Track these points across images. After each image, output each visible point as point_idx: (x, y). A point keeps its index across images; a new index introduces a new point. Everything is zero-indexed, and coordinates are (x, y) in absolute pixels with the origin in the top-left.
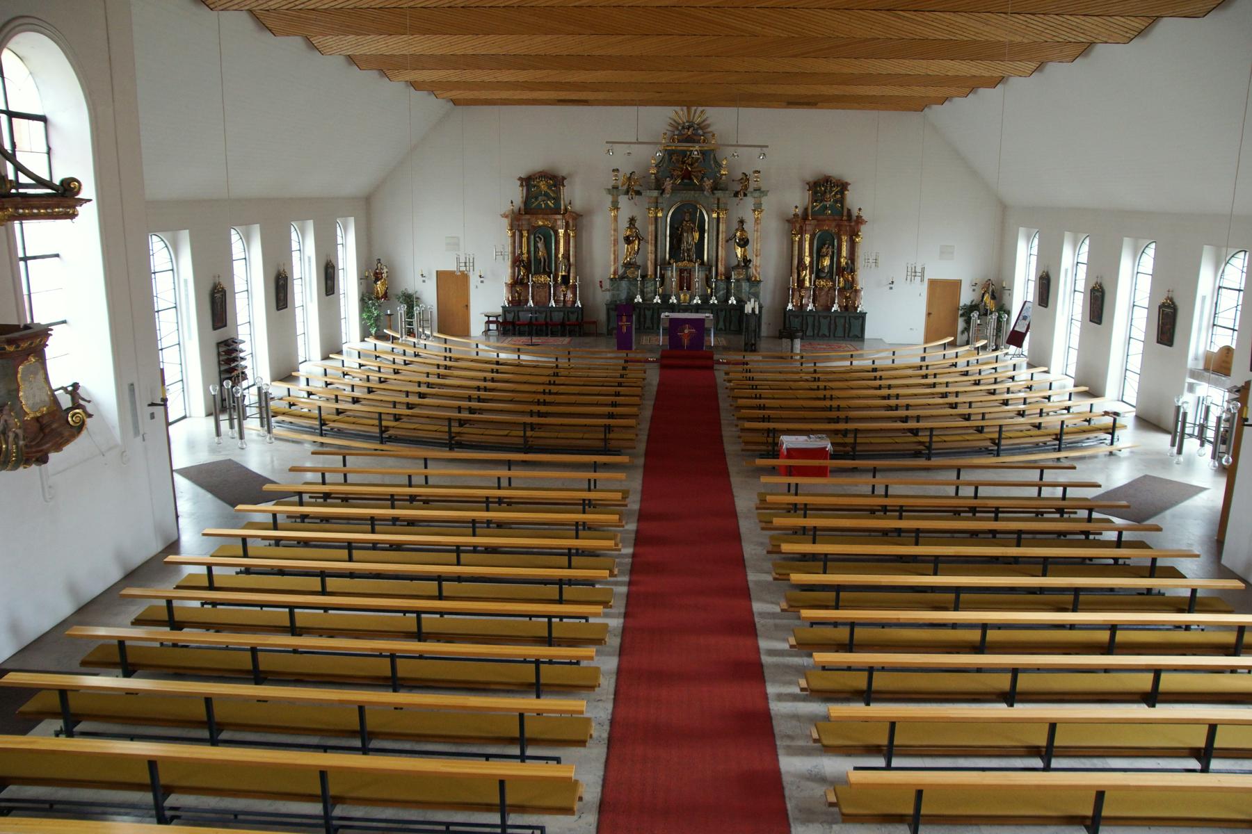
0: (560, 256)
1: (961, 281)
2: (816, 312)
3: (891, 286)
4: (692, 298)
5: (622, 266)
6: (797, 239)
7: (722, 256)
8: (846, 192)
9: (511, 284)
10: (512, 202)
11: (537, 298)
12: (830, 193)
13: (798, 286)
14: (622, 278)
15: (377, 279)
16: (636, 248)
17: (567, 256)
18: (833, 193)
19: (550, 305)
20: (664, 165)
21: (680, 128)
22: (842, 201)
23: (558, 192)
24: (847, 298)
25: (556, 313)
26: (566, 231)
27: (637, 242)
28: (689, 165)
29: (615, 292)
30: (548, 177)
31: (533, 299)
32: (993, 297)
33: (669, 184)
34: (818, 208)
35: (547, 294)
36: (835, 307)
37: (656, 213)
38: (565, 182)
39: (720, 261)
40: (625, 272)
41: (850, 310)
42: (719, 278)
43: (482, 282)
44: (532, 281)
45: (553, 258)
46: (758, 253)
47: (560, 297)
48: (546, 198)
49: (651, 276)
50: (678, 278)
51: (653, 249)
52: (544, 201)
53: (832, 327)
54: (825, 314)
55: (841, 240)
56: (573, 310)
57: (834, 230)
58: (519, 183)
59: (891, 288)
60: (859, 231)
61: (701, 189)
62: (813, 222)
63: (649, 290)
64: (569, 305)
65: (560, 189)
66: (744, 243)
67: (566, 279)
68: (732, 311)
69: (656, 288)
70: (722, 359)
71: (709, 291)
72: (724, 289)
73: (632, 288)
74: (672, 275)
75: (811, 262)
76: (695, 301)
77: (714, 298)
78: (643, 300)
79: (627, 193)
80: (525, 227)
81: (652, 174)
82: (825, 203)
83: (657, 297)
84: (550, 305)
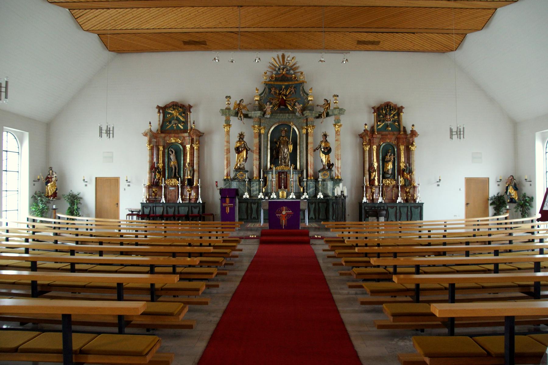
0: (187, 165)
1: (488, 178)
2: (385, 203)
3: (438, 183)
4: (288, 194)
5: (234, 171)
6: (368, 149)
7: (311, 162)
8: (402, 114)
9: (149, 186)
10: (150, 123)
11: (169, 197)
12: (390, 115)
13: (369, 184)
14: (234, 179)
15: (47, 183)
16: (245, 156)
17: (192, 164)
18: (392, 115)
19: (178, 202)
20: (266, 96)
21: (277, 69)
22: (399, 121)
23: (186, 117)
24: (406, 193)
25: (183, 208)
26: (191, 146)
27: (245, 152)
28: (284, 95)
30: (178, 106)
31: (165, 197)
32: (516, 188)
33: (268, 108)
34: (381, 126)
35: (177, 194)
36: (399, 200)
37: (260, 130)
38: (191, 110)
39: (309, 165)
40: (236, 175)
41: (410, 202)
42: (309, 178)
43: (129, 185)
44: (165, 183)
45: (182, 167)
46: (339, 158)
47: (187, 196)
48: (177, 122)
49: (256, 177)
50: (277, 179)
51: (258, 157)
52: (176, 124)
53: (398, 215)
54: (392, 205)
55: (400, 149)
56: (196, 205)
57: (394, 143)
58: (157, 110)
59: (438, 185)
60: (413, 142)
61: (294, 112)
62: (378, 136)
63: (254, 188)
64: (192, 201)
65: (188, 114)
66: (328, 151)
67: (191, 182)
68: (320, 204)
69: (260, 187)
70: (318, 235)
72: (313, 188)
74: (272, 178)
75: (379, 166)
76: (291, 197)
77: (305, 194)
78: (250, 196)
79: (236, 114)
80: (162, 143)
81: (256, 100)
82: (386, 122)
83: (261, 194)
84: (178, 202)
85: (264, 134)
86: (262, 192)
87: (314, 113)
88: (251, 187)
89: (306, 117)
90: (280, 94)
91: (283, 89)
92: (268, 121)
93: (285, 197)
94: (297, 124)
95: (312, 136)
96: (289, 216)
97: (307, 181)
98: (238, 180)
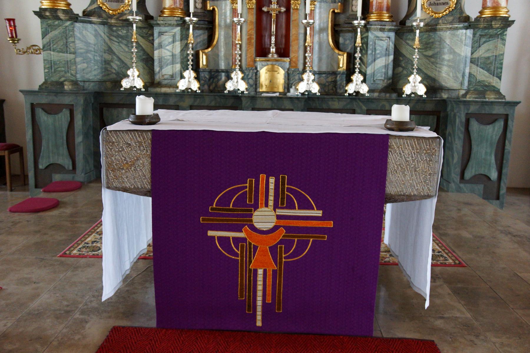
29: (55, 56)
42: (373, 18)
49: (172, 10)
50: (253, 18)
71: (343, 60)
73: (115, 47)
77: (357, 78)
86: (196, 68)
88: (153, 50)
93: (281, 90)
96: (302, 245)
97: (366, 28)
98: (100, 16)
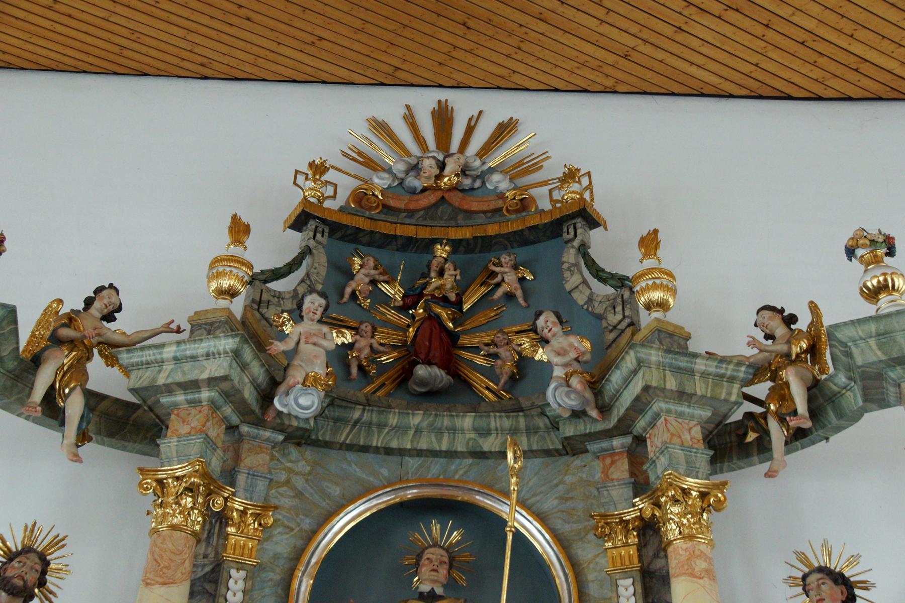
28: (444, 301)
85: (253, 573)
87: (704, 375)
89: (623, 427)
90: (412, 299)
91: (435, 263)
92: (303, 466)
94: (550, 504)
95: (710, 573)
